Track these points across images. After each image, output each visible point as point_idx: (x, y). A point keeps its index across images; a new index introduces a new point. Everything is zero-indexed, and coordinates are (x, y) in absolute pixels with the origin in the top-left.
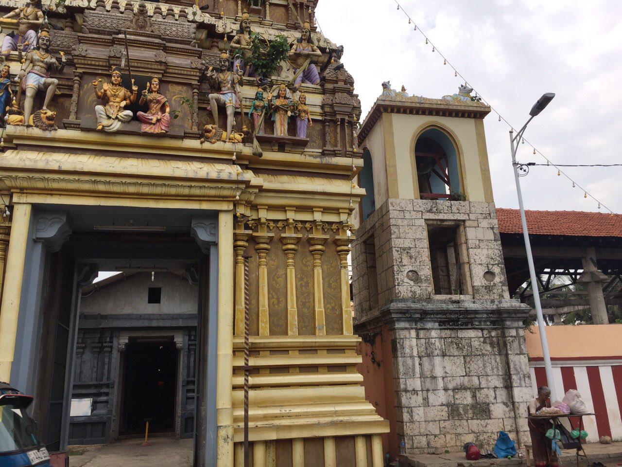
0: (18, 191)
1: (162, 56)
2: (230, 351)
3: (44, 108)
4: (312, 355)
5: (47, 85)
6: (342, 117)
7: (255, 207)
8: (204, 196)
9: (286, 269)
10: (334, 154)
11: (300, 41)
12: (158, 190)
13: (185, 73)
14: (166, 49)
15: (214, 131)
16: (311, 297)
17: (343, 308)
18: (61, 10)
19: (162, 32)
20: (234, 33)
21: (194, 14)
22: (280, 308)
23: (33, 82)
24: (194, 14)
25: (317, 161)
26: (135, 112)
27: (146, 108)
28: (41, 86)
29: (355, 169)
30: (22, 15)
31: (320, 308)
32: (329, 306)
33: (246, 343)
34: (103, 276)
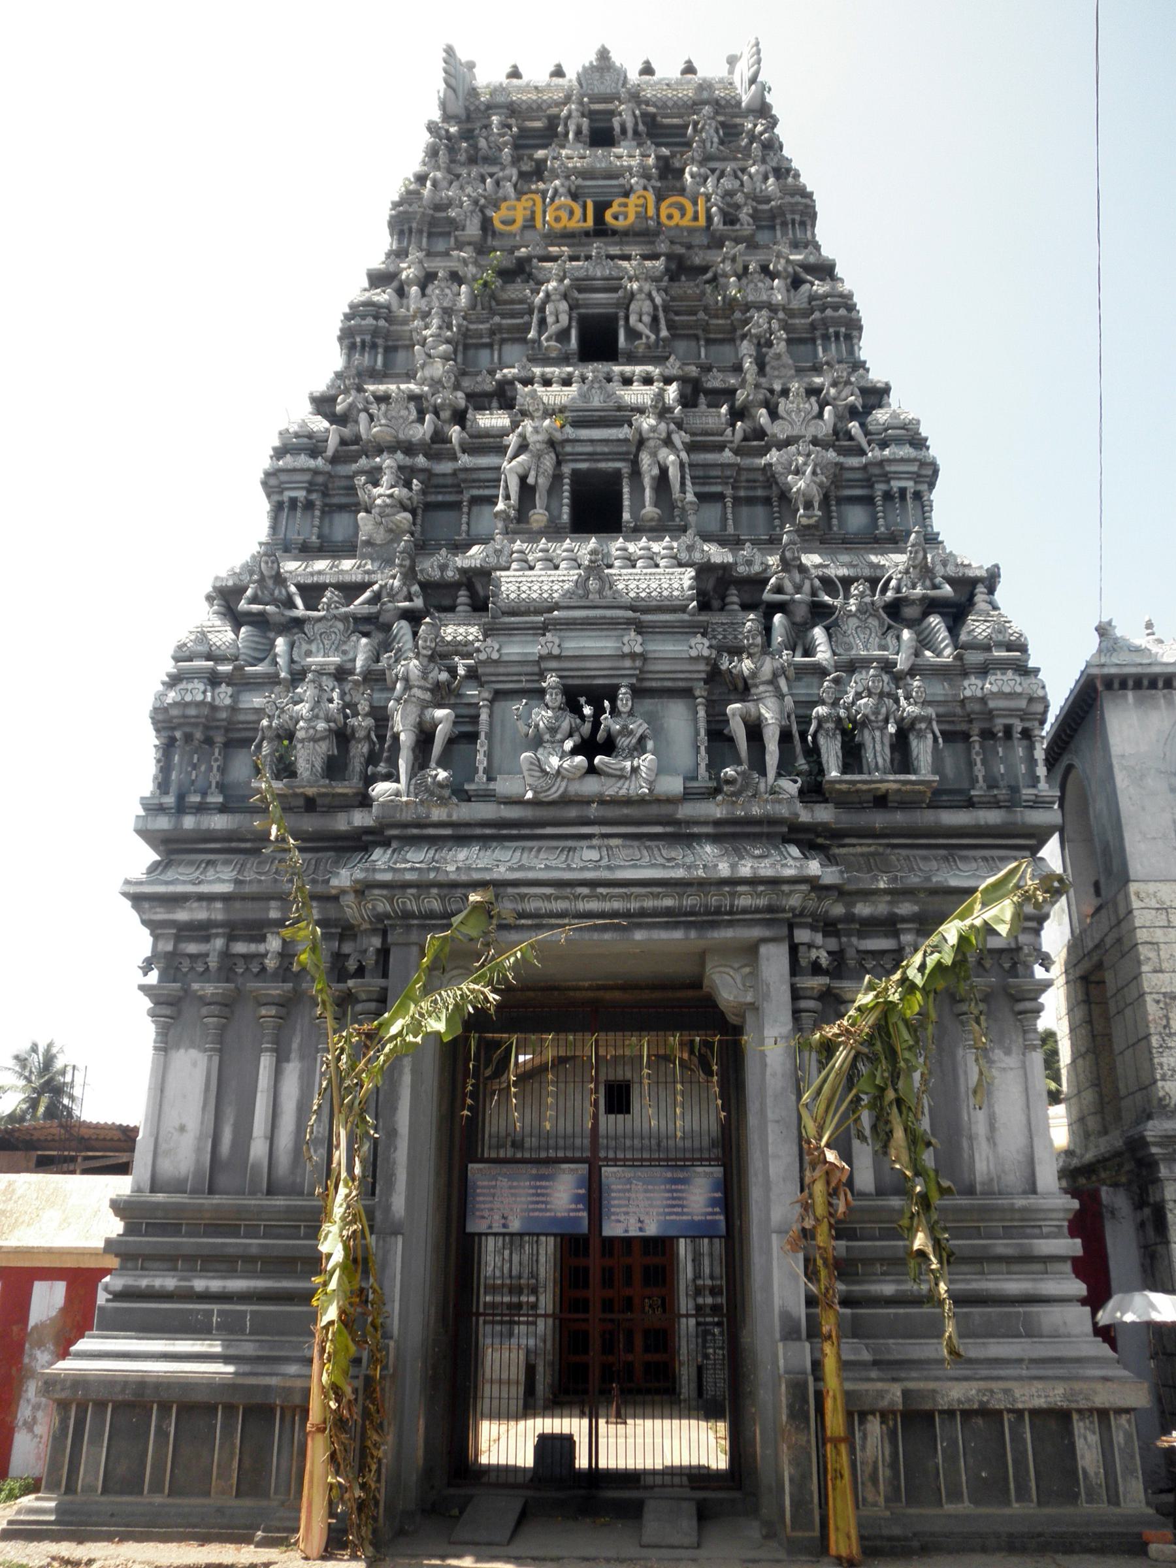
1: (633, 642)
3: (433, 765)
14: (641, 628)
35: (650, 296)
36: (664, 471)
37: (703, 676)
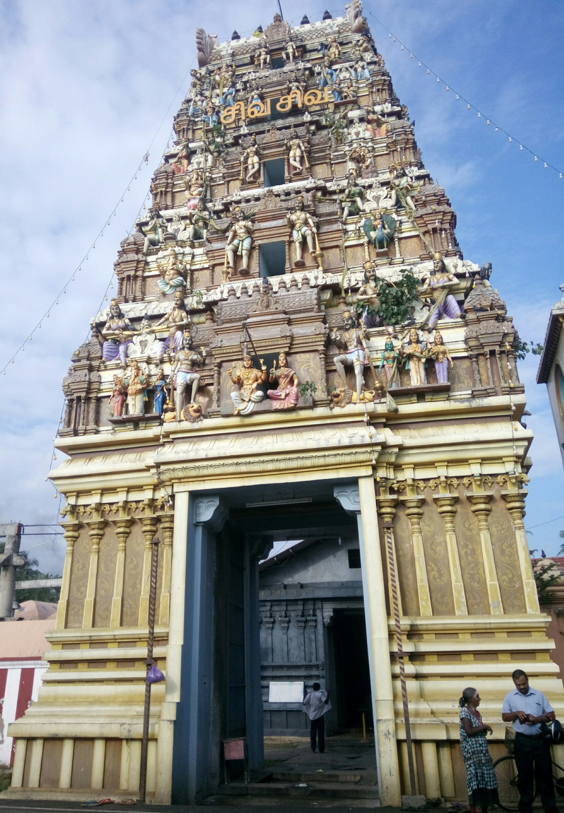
0: (177, 481)
2: (385, 635)
4: (487, 639)
5: (192, 381)
6: (491, 348)
7: (397, 467)
8: (340, 464)
9: (445, 535)
10: (487, 394)
11: (433, 273)
12: (294, 464)
13: (310, 340)
14: (290, 322)
15: (342, 394)
16: (480, 566)
17: (523, 579)
18: (201, 307)
19: (286, 306)
20: (360, 284)
21: (316, 278)
22: (442, 583)
23: (181, 379)
24: (316, 278)
25: (465, 405)
26: (265, 392)
27: (274, 384)
28: (188, 382)
29: (514, 408)
30: (171, 319)
31: (492, 582)
32: (504, 577)
33: (397, 625)
34: (280, 547)
35: (299, 146)
36: (304, 237)
37: (323, 343)
